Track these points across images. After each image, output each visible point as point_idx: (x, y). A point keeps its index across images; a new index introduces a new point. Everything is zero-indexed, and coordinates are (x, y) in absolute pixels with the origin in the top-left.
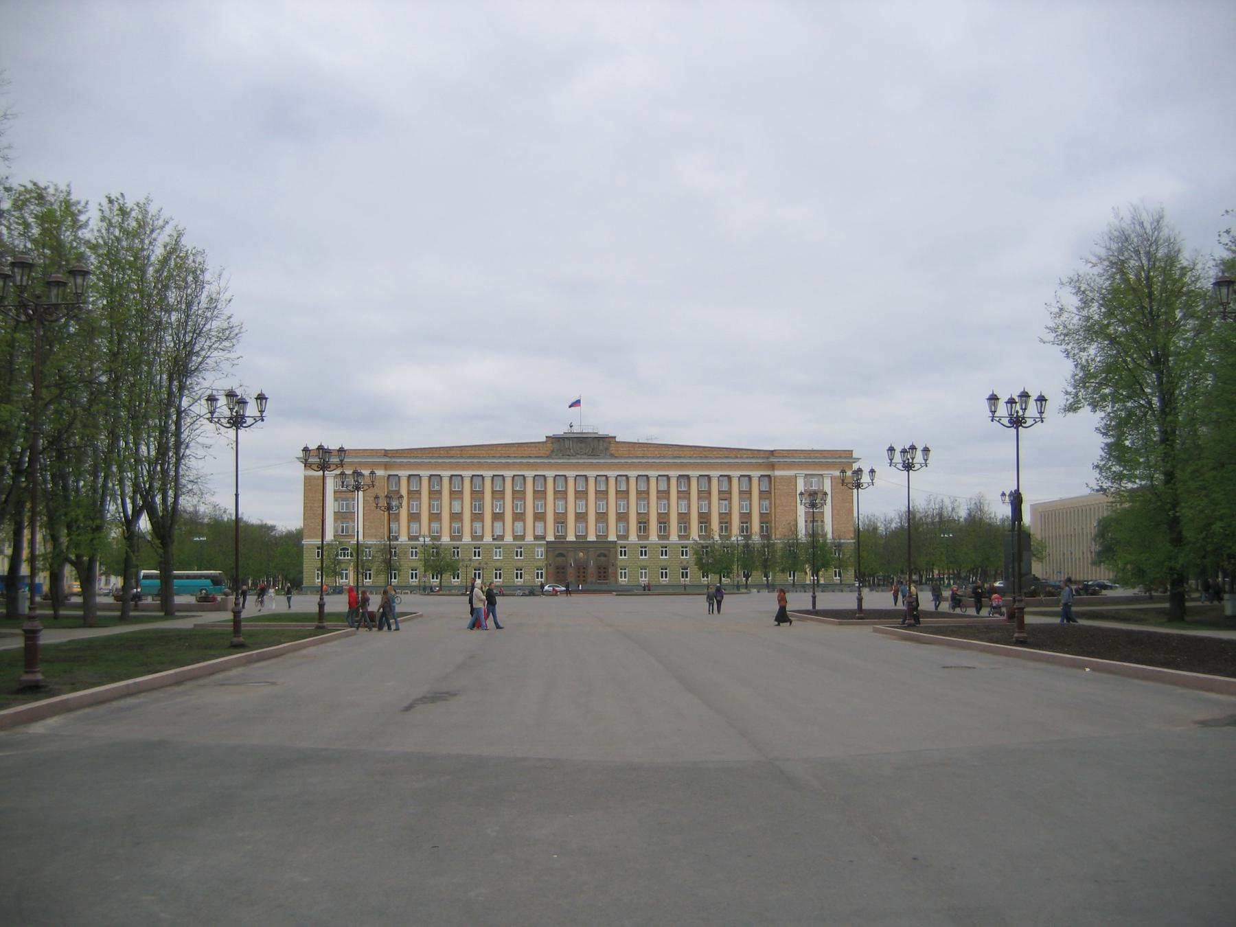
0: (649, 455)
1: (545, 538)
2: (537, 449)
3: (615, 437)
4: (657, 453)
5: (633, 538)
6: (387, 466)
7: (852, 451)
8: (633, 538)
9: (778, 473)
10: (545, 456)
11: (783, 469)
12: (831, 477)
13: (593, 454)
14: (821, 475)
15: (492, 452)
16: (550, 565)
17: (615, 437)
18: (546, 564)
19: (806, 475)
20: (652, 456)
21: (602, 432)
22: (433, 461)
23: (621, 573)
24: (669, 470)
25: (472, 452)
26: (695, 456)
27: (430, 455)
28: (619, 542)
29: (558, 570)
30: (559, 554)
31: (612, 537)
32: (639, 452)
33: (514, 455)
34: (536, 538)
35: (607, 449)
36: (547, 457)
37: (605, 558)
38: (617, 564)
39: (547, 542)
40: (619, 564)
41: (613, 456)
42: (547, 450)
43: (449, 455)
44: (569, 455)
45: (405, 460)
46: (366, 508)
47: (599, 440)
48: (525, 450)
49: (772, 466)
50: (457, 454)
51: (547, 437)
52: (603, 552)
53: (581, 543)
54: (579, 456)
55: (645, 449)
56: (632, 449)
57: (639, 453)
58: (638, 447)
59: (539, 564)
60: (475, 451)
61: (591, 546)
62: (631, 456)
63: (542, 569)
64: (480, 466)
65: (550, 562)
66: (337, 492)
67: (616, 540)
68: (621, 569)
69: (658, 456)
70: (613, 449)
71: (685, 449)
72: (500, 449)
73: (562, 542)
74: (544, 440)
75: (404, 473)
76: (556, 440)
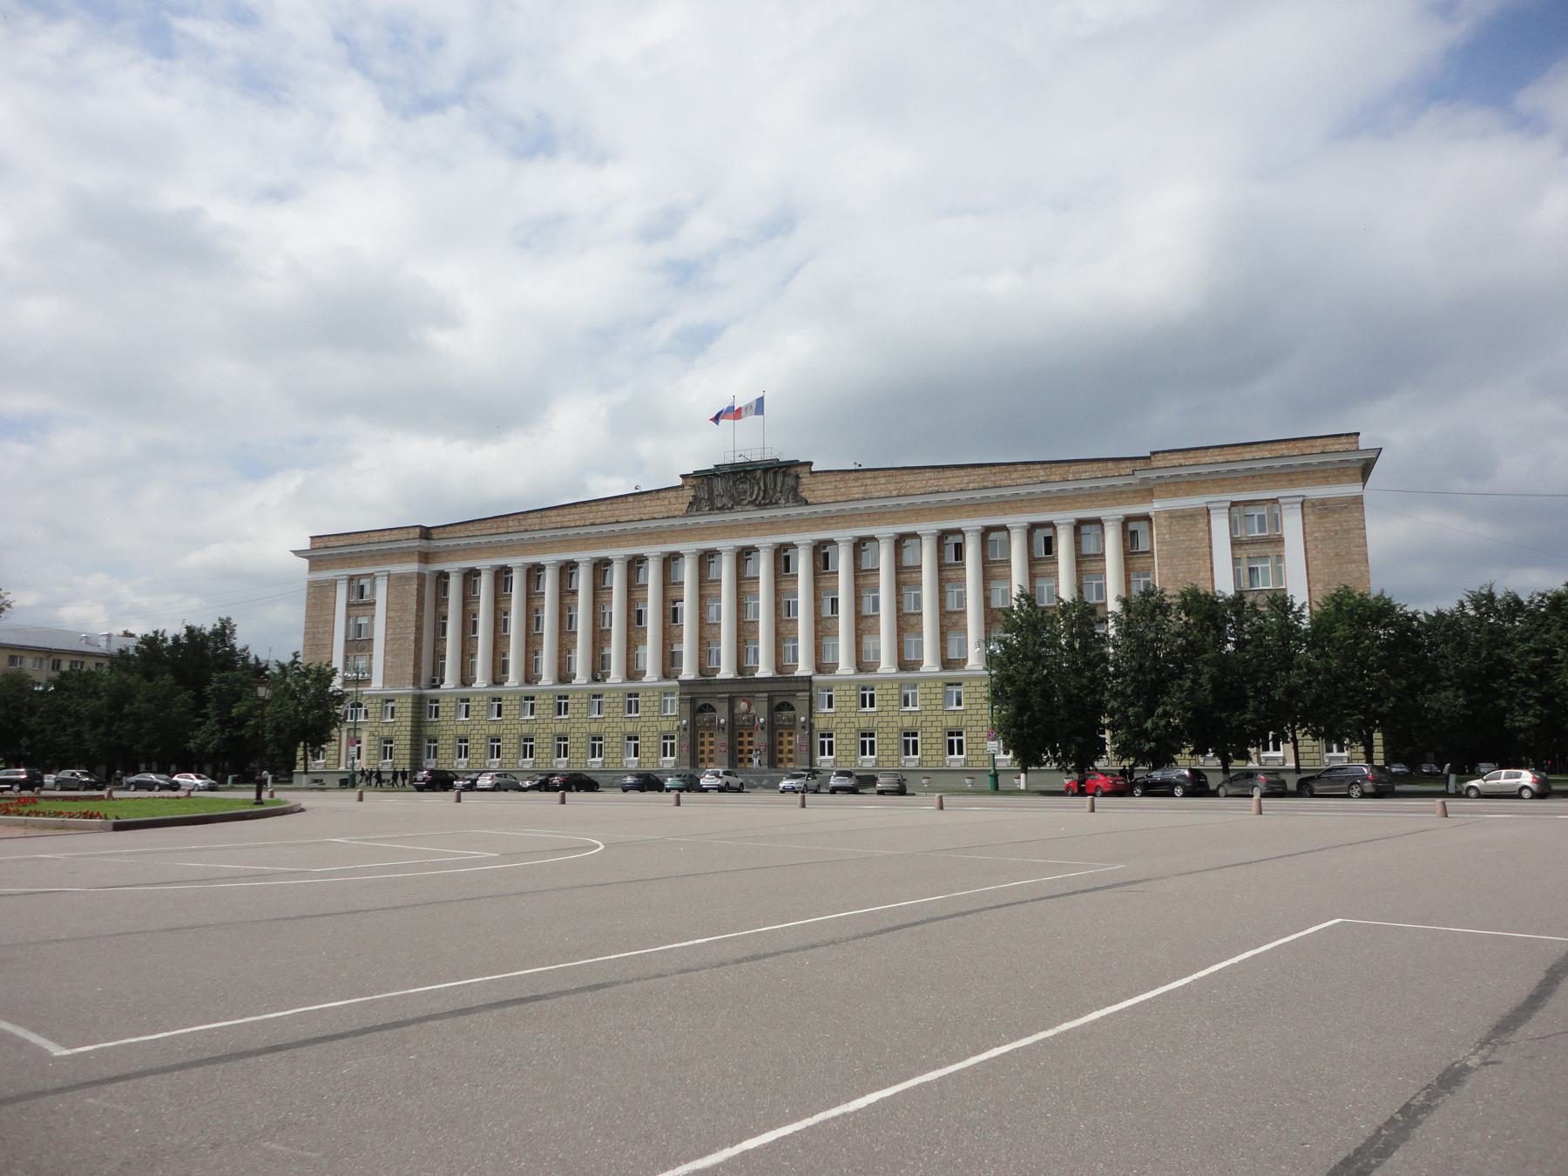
0: (877, 494)
1: (677, 677)
2: (666, 502)
3: (810, 464)
4: (891, 487)
5: (845, 667)
6: (425, 557)
7: (1358, 434)
8: (845, 667)
9: (1154, 507)
10: (680, 513)
11: (1175, 495)
12: (1302, 504)
13: (766, 502)
14: (1275, 501)
15: (591, 516)
16: (685, 729)
17: (810, 464)
18: (678, 727)
19: (1233, 504)
20: (883, 494)
21: (785, 457)
22: (494, 539)
23: (823, 743)
24: (918, 521)
25: (559, 519)
26: (971, 486)
27: (493, 531)
28: (817, 678)
29: (750, 739)
30: (705, 706)
31: (803, 668)
32: (856, 490)
33: (626, 519)
34: (666, 676)
35: (795, 490)
36: (687, 514)
37: (790, 713)
38: (811, 726)
39: (679, 681)
40: (816, 726)
41: (807, 503)
42: (682, 503)
43: (522, 528)
44: (718, 509)
45: (452, 543)
46: (389, 632)
47: (776, 472)
48: (645, 506)
49: (1147, 492)
50: (535, 525)
51: (683, 476)
52: (785, 700)
53: (745, 681)
54: (739, 508)
55: (869, 482)
56: (841, 485)
57: (857, 492)
58: (857, 479)
59: (665, 727)
60: (564, 516)
61: (762, 687)
62: (839, 498)
63: (672, 738)
64: (570, 543)
65: (684, 722)
66: (354, 605)
67: (810, 673)
68: (823, 736)
69: (895, 493)
70: (807, 487)
71: (948, 473)
72: (602, 508)
73: (708, 683)
74: (680, 482)
75: (454, 567)
76: (703, 479)
